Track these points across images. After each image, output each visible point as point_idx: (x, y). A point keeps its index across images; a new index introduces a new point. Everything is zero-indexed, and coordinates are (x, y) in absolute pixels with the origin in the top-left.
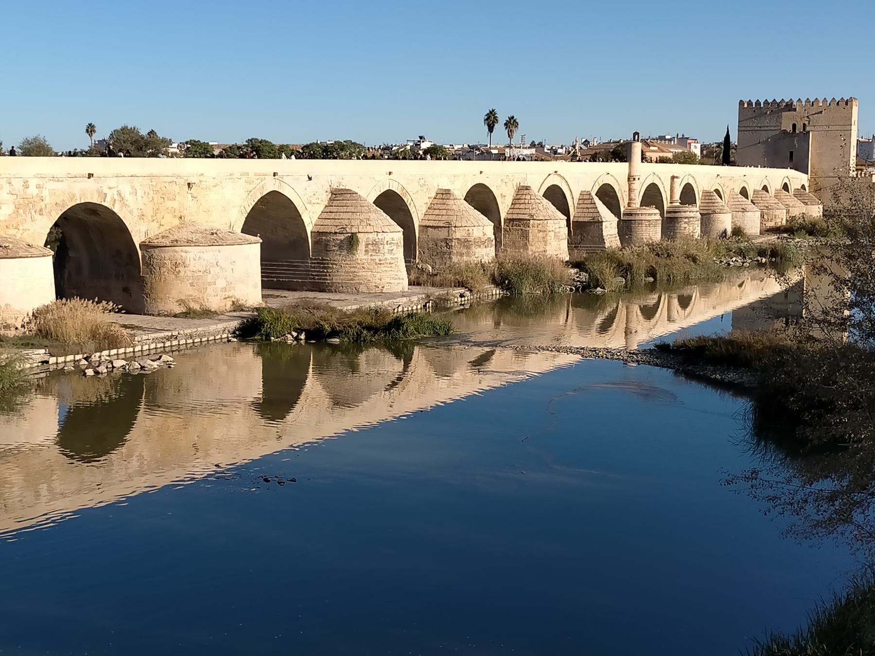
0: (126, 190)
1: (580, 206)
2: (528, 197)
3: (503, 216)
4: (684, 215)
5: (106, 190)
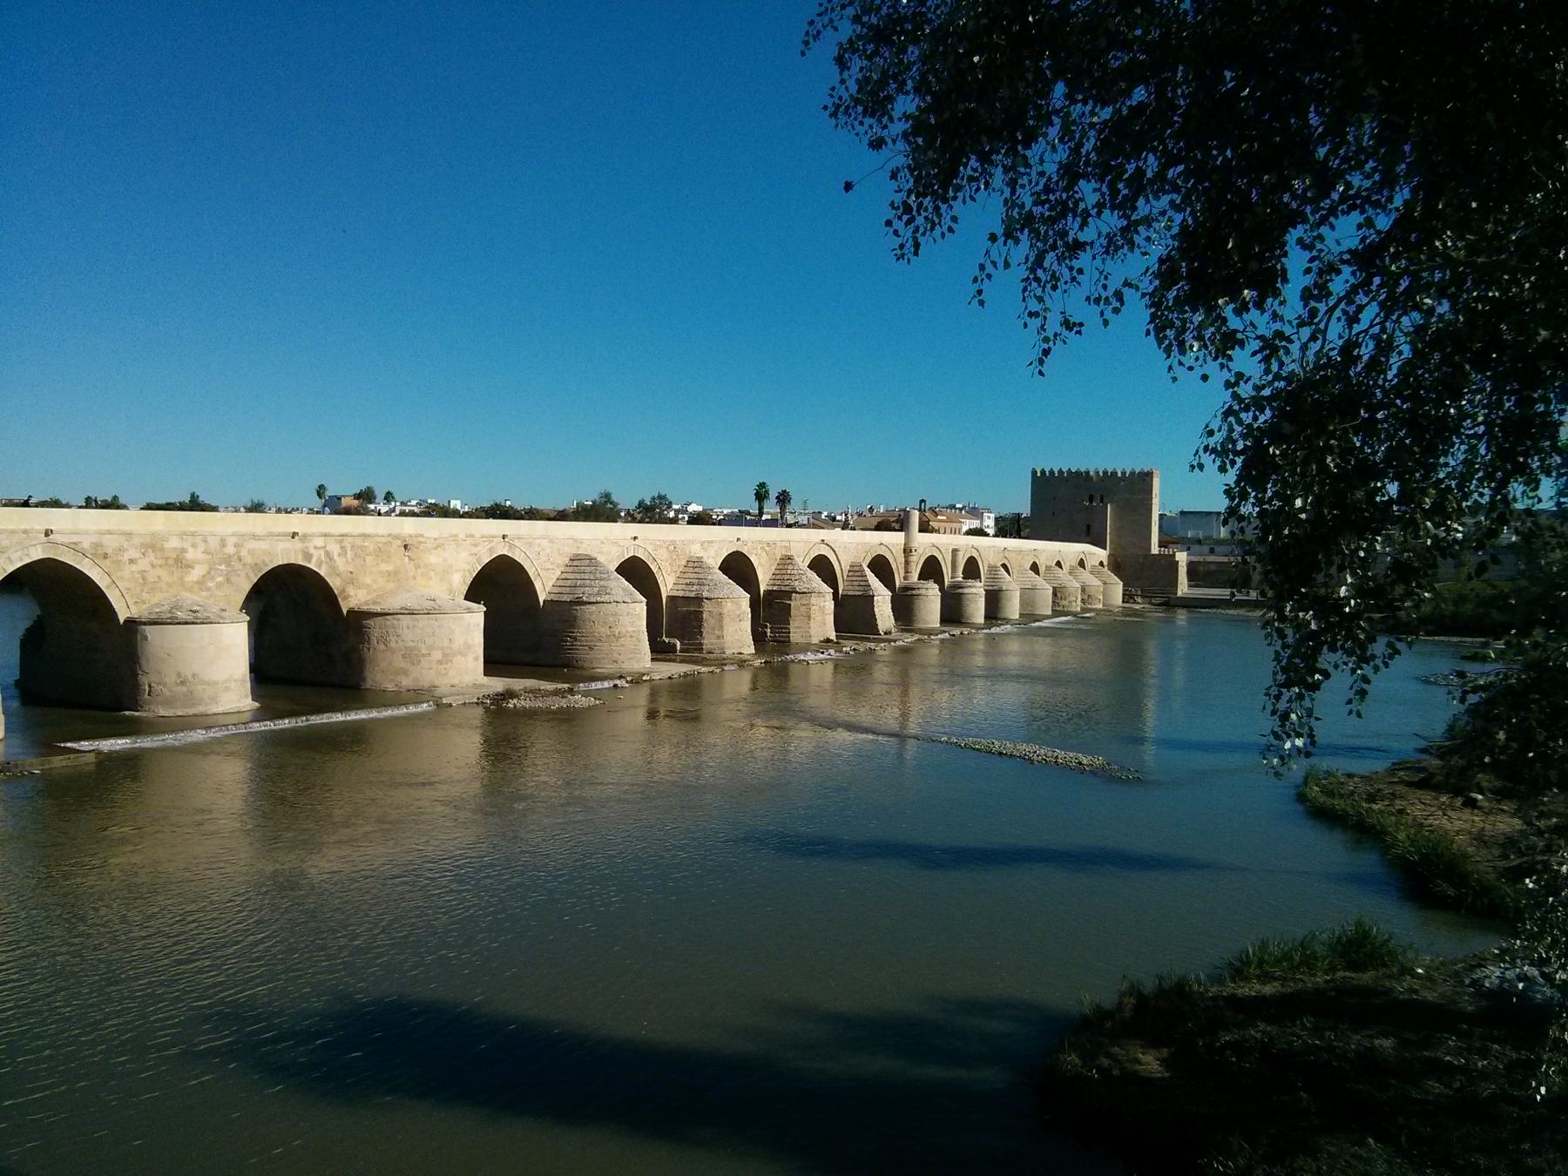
0: (334, 548)
1: (850, 579)
2: (790, 567)
3: (763, 588)
4: (966, 591)
5: (312, 551)
